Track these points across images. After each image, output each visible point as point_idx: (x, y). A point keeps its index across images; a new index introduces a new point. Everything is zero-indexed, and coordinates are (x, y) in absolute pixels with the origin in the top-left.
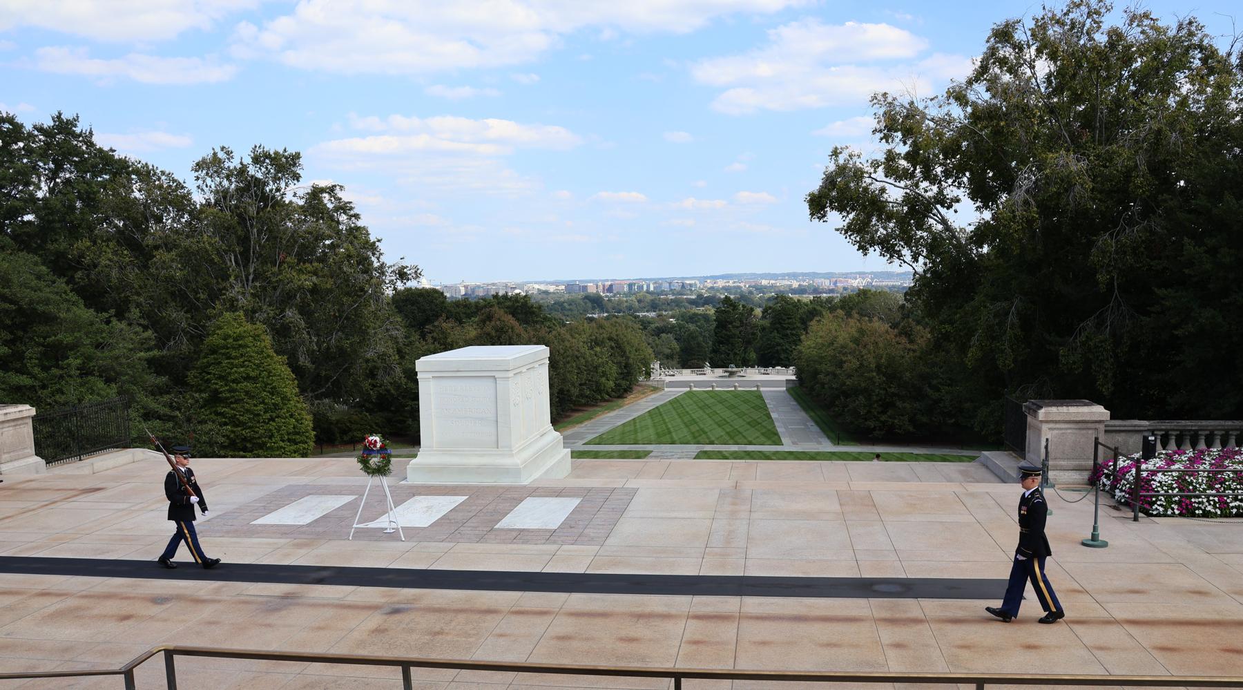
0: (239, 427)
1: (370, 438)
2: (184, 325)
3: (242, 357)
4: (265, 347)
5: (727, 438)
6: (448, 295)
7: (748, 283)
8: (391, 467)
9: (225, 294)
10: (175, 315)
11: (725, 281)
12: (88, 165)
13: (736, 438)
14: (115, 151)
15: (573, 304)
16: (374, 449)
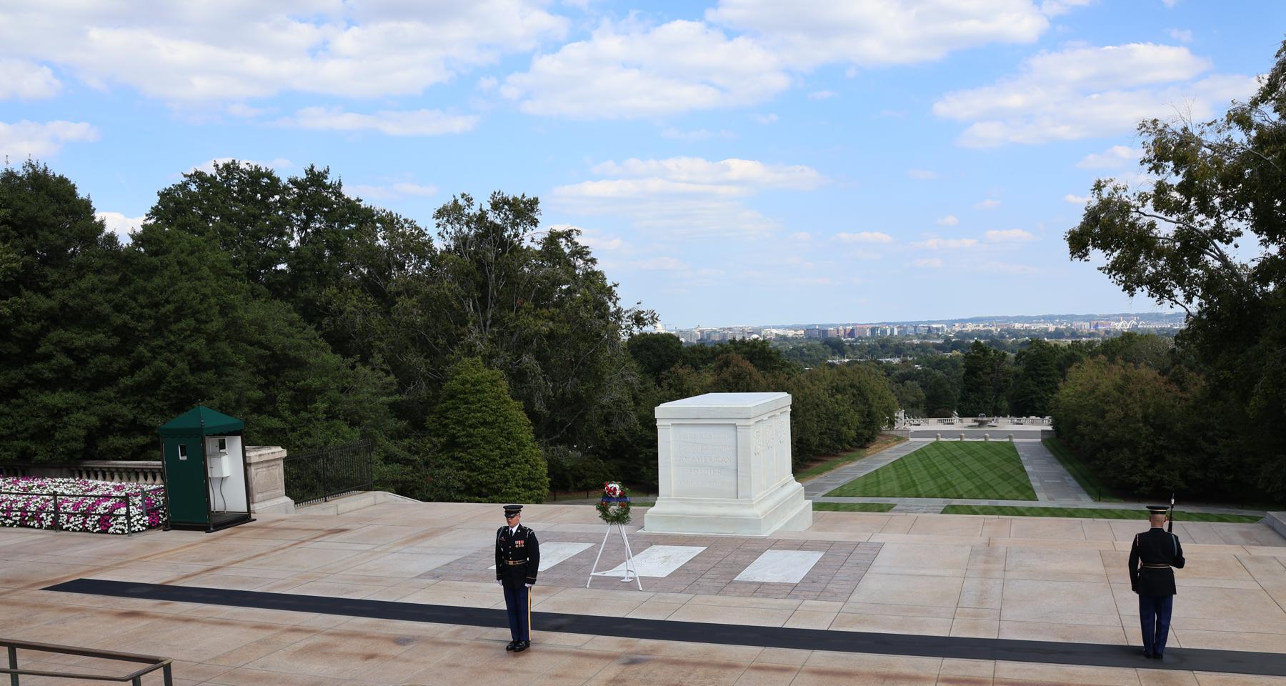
1: (610, 486)
2: (423, 370)
4: (502, 392)
5: (977, 492)
6: (683, 340)
7: (999, 326)
9: (463, 340)
10: (415, 360)
11: (975, 325)
12: (337, 216)
13: (987, 492)
14: (361, 200)
16: (614, 496)
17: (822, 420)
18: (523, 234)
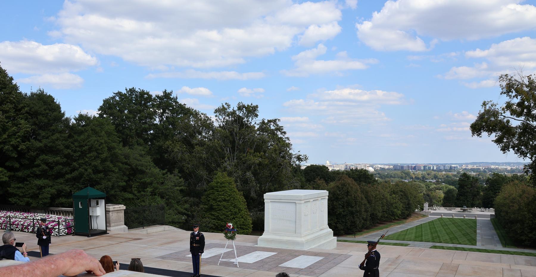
0: (220, 221)
1: (228, 224)
4: (233, 187)
5: (449, 240)
6: (330, 169)
11: (472, 166)
13: (454, 241)
14: (186, 105)
15: (396, 174)
17: (384, 205)
18: (252, 120)
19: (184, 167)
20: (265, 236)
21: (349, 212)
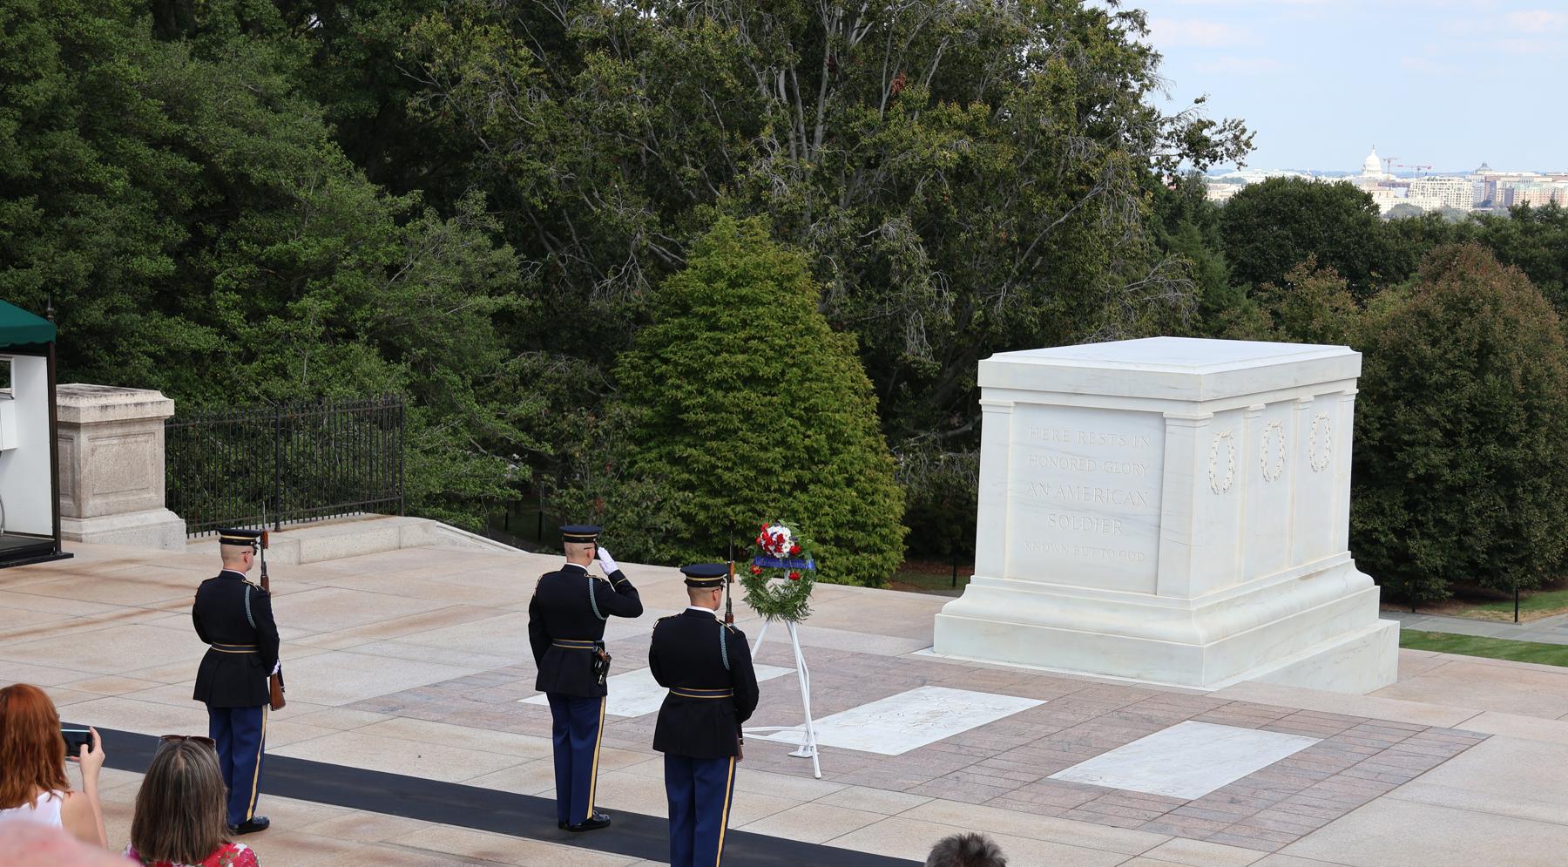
0: (724, 496)
1: (770, 531)
3: (744, 328)
6: (1386, 203)
8: (809, 601)
9: (744, 170)
10: (622, 212)
16: (777, 555)
19: (520, 173)
20: (977, 597)
21: (1489, 468)
